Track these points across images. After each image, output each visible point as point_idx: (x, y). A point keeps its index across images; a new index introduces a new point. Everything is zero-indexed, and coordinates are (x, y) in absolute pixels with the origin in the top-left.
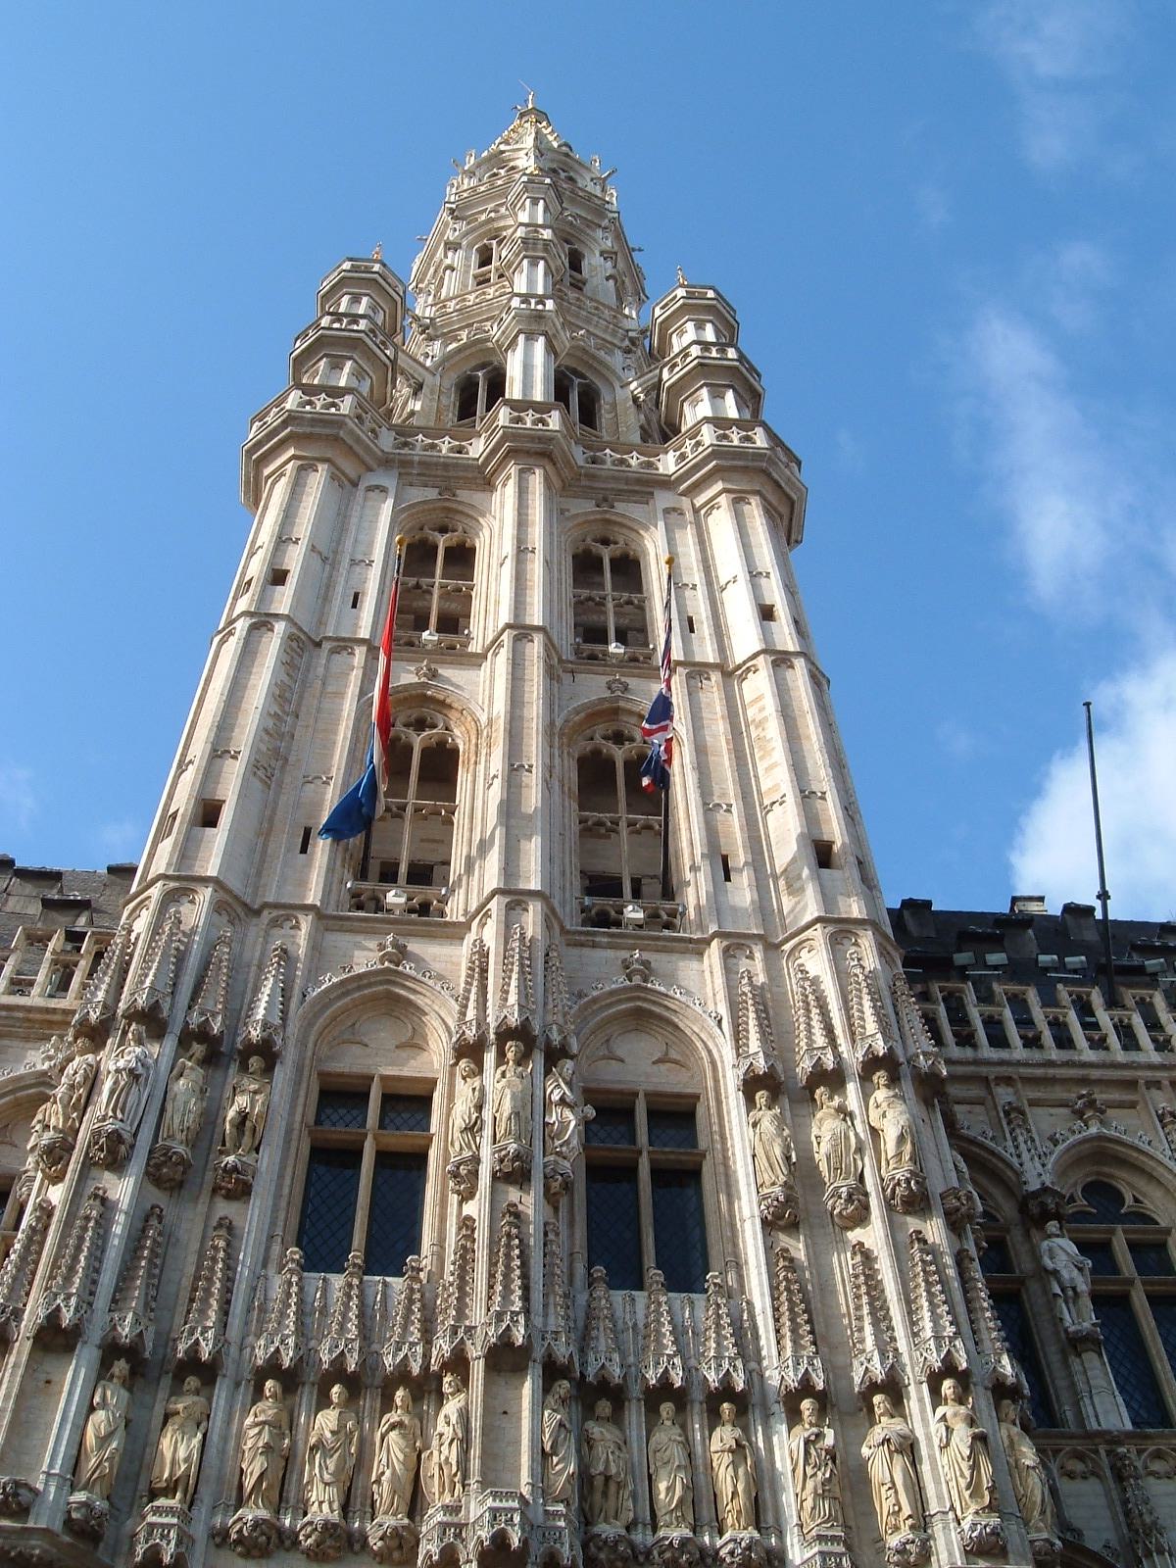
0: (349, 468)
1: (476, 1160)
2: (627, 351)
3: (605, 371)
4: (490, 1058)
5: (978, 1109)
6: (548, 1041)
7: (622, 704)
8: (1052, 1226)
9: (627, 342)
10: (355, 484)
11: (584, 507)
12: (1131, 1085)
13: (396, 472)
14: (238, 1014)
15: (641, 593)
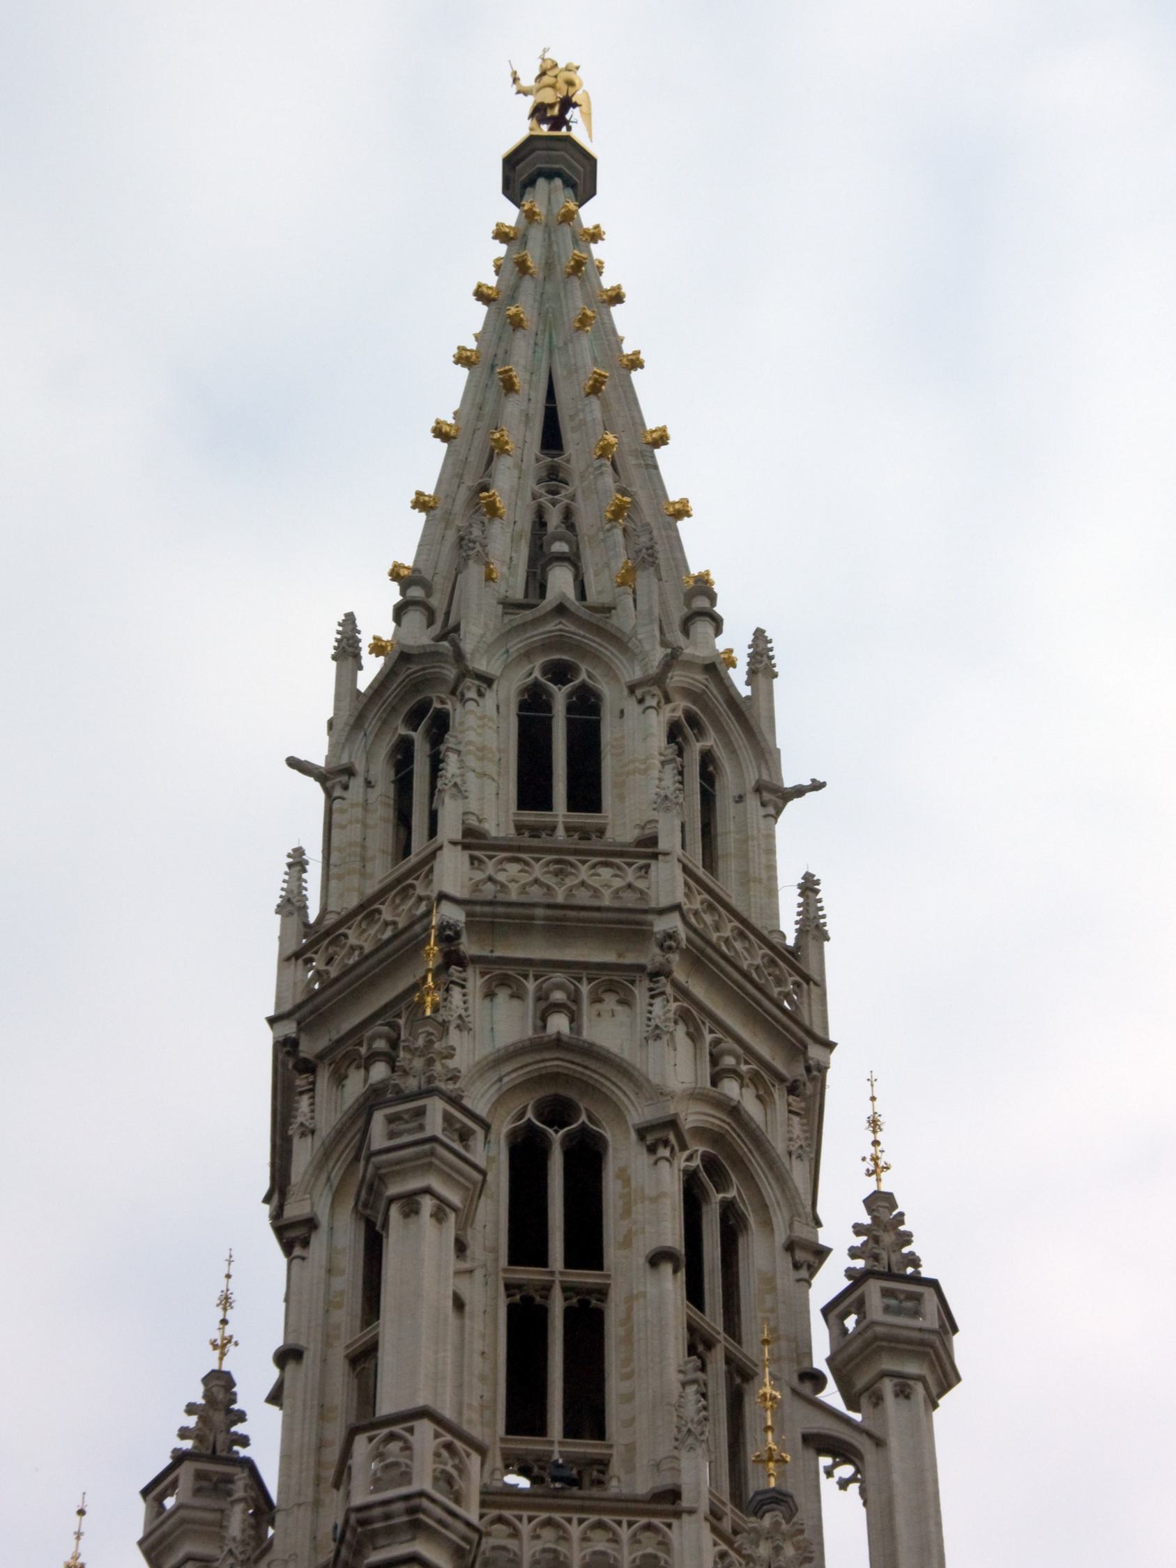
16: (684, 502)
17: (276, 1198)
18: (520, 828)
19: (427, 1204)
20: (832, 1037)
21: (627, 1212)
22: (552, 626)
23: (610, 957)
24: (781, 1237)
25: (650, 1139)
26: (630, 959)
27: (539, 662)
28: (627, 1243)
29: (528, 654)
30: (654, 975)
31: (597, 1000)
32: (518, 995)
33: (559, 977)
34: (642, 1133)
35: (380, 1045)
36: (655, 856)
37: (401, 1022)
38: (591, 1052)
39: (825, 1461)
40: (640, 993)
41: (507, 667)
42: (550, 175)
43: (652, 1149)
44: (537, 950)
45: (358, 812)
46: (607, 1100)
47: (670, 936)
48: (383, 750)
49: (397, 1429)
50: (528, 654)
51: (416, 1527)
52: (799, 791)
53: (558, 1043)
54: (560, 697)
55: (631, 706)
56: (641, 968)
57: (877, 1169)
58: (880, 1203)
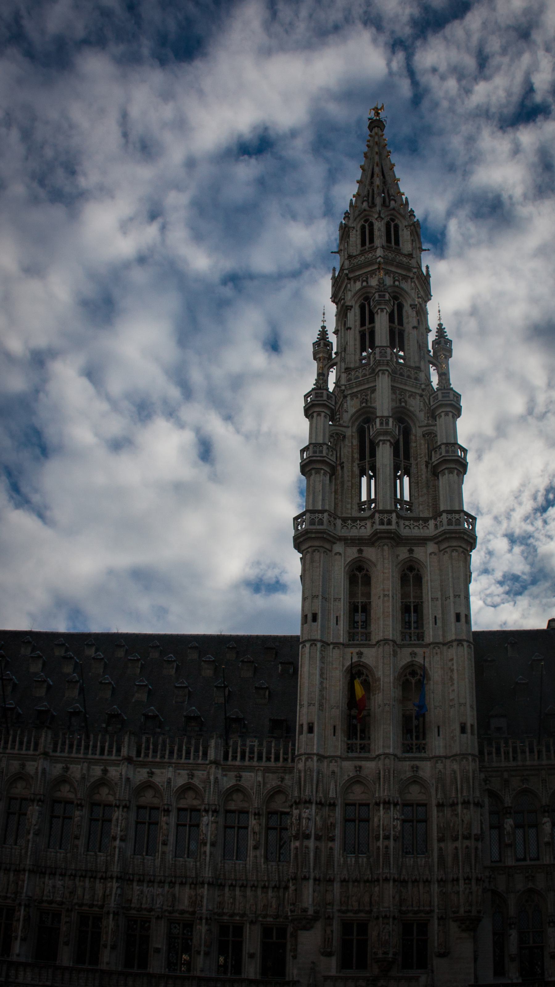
0: (327, 546)
1: (379, 834)
2: (421, 396)
4: (382, 806)
6: (394, 802)
7: (414, 663)
10: (331, 551)
11: (403, 553)
13: (343, 543)
15: (422, 600)
16: (404, 193)
17: (333, 298)
18: (387, 246)
19: (385, 311)
20: (432, 294)
21: (408, 318)
22: (392, 212)
24: (424, 327)
25: (412, 307)
26: (408, 275)
27: (389, 217)
28: (408, 323)
29: (388, 216)
30: (412, 278)
31: (402, 280)
32: (389, 276)
33: (397, 275)
34: (411, 305)
35: (364, 279)
36: (413, 258)
38: (402, 289)
39: (431, 366)
40: (409, 280)
41: (385, 217)
43: (412, 309)
44: (393, 269)
45: (355, 236)
46: (404, 298)
47: (416, 272)
48: (359, 226)
49: (384, 348)
50: (388, 216)
51: (388, 365)
52: (425, 250)
53: (397, 286)
54: (392, 224)
55: (405, 230)
56: (409, 277)
58: (440, 325)
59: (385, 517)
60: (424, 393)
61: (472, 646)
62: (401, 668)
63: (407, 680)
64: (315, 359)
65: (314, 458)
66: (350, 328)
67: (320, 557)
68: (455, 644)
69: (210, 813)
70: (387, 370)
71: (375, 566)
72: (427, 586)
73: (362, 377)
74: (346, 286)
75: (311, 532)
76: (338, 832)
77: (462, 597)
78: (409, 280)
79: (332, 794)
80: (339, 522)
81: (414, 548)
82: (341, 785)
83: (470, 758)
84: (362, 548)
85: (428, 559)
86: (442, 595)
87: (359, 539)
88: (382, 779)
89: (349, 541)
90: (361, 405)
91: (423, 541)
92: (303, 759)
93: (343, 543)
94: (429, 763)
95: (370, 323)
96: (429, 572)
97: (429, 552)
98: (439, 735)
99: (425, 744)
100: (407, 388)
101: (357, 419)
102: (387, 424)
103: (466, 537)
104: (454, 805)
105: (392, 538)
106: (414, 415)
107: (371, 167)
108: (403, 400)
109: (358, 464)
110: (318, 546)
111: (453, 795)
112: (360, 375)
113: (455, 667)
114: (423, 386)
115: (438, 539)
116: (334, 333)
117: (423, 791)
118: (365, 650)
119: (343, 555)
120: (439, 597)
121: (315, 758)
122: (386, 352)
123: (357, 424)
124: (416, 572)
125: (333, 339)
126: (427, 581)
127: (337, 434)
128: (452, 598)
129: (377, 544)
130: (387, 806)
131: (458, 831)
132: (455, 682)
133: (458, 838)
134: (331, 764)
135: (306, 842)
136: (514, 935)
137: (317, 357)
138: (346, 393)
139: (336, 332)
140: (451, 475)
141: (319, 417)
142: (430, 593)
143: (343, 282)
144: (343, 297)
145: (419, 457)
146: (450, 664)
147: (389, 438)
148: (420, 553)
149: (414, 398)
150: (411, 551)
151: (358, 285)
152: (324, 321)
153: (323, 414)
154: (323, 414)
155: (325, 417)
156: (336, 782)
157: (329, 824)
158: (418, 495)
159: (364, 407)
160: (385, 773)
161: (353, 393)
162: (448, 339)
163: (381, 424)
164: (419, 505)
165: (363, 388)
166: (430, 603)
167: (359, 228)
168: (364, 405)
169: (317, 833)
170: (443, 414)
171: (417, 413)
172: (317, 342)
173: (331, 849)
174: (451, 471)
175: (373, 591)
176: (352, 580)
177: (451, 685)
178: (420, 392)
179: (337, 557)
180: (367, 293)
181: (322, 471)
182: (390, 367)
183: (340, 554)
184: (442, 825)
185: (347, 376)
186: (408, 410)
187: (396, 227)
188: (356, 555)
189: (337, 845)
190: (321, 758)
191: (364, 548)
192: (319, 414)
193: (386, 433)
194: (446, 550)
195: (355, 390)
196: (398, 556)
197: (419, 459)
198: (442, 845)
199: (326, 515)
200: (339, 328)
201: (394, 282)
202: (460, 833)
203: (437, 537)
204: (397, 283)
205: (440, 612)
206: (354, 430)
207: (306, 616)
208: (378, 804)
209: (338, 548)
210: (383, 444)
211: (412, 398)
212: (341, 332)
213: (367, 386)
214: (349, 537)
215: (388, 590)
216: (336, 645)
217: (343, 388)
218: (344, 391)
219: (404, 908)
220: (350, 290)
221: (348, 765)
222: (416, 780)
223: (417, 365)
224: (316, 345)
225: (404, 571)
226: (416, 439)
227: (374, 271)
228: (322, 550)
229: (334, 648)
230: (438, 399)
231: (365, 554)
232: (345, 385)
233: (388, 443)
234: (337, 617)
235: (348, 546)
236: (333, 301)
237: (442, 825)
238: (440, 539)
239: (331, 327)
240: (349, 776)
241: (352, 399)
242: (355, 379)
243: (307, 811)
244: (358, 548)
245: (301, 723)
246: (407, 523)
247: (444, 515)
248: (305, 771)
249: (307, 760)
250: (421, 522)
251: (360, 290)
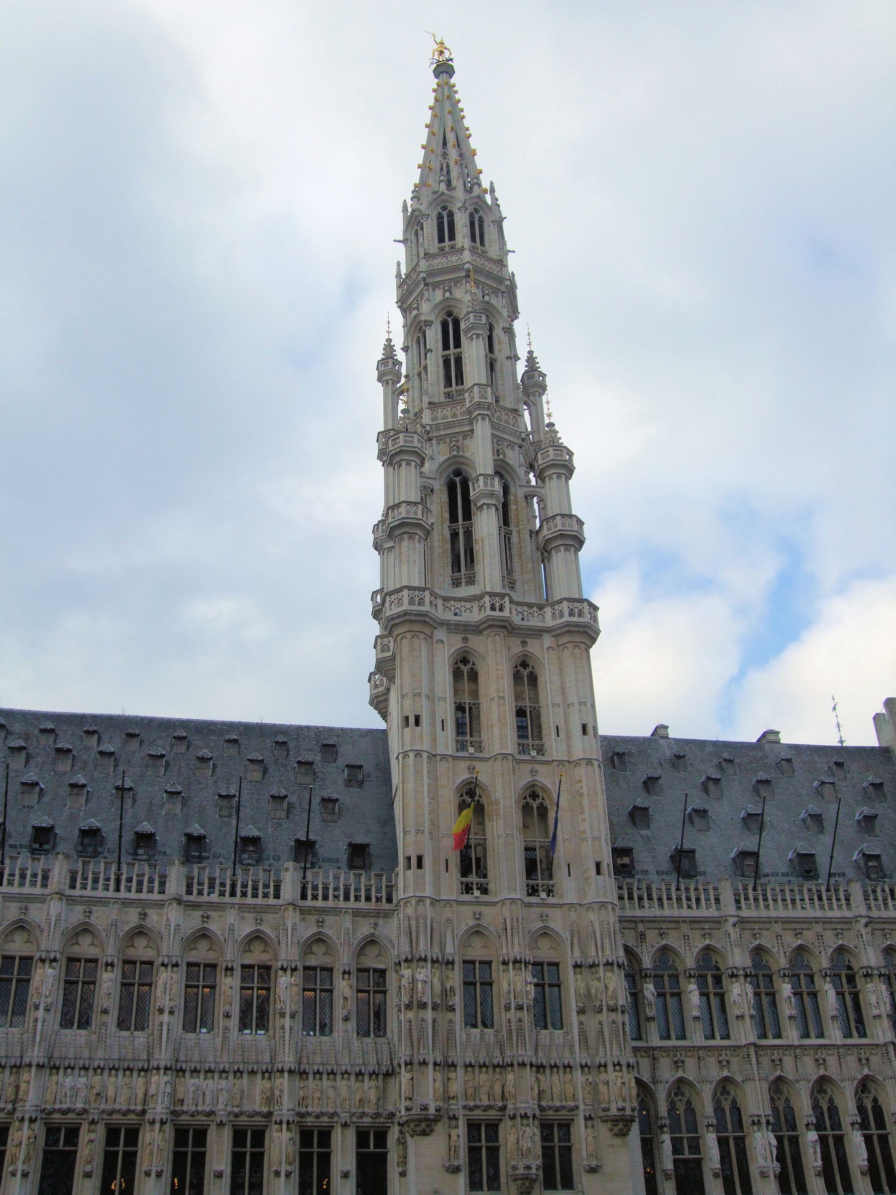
0: (428, 631)
2: (521, 447)
3: (508, 469)
5: (633, 931)
7: (536, 783)
8: (648, 980)
9: (520, 441)
10: (431, 637)
12: (678, 922)
13: (445, 628)
14: (442, 948)
17: (400, 304)
23: (495, 285)
26: (498, 287)
30: (502, 292)
33: (486, 287)
34: (503, 329)
37: (452, 284)
38: (493, 306)
42: (447, 73)
48: (435, 213)
54: (477, 216)
55: (492, 225)
57: (530, 344)
58: (531, 353)
59: (497, 602)
60: (523, 444)
61: (602, 765)
62: (522, 789)
63: (527, 803)
64: (380, 380)
65: (408, 520)
66: (431, 351)
67: (420, 645)
68: (583, 763)
69: (289, 972)
70: (488, 415)
71: (484, 658)
72: (546, 688)
73: (452, 418)
74: (421, 294)
75: (410, 614)
76: (457, 1000)
77: (589, 705)
78: (500, 295)
79: (449, 949)
80: (440, 602)
81: (527, 640)
82: (459, 936)
83: (610, 907)
84: (467, 636)
85: (546, 654)
86: (564, 701)
87: (465, 626)
88: (509, 931)
89: (453, 628)
90: (450, 453)
91: (539, 632)
92: (413, 902)
93: (445, 628)
94: (559, 910)
95: (455, 347)
96: (547, 672)
97: (546, 647)
98: (569, 875)
99: (553, 886)
100: (504, 436)
101: (446, 469)
102: (492, 485)
103: (590, 632)
104: (593, 966)
105: (505, 627)
106: (514, 470)
107: (442, 130)
108: (501, 451)
109: (449, 527)
110: (417, 632)
111: (594, 953)
112: (449, 414)
113: (585, 790)
114: (523, 436)
115: (556, 632)
116: (402, 349)
117: (554, 946)
118: (479, 765)
119: (446, 643)
120: (561, 702)
121: (428, 902)
122: (486, 392)
123: (445, 475)
124: (530, 669)
125: (401, 356)
126: (546, 681)
127: (424, 487)
128: (576, 705)
129: (485, 633)
130: (517, 965)
131: (602, 1001)
132: (586, 808)
133: (602, 1009)
134: (445, 909)
135: (422, 1013)
136: (666, 1139)
137: (384, 379)
138: (430, 435)
139: (405, 349)
140: (567, 553)
141: (408, 467)
142: (549, 698)
143: (417, 285)
144: (416, 305)
145: (521, 523)
146: (578, 786)
147: (494, 502)
148: (534, 647)
149: (513, 449)
150: (524, 643)
151: (438, 296)
152: (389, 332)
153: (413, 464)
154: (413, 464)
155: (416, 467)
156: (453, 933)
157: (449, 988)
158: (522, 571)
159: (455, 456)
160: (512, 923)
161: (441, 435)
162: (540, 372)
163: (485, 484)
164: (523, 584)
165: (453, 431)
166: (551, 710)
167: (435, 218)
168: (455, 453)
169: (434, 1001)
170: (554, 476)
171: (516, 467)
172: (383, 359)
173: (451, 1021)
174: (567, 547)
175: (482, 690)
176: (457, 675)
177: (581, 813)
178: (520, 441)
179: (439, 645)
180: (450, 306)
181: (417, 537)
182: (490, 411)
183: (442, 642)
184: (582, 992)
185: (432, 413)
186: (507, 464)
187: (481, 220)
188: (460, 645)
189: (458, 1017)
190: (434, 902)
191: (470, 637)
192: (408, 463)
193: (492, 495)
194: (567, 645)
195: (442, 433)
196: (509, 648)
197: (521, 527)
198: (583, 1018)
199: (427, 593)
200: (410, 345)
201: (483, 297)
202: (604, 1003)
203: (556, 629)
204: (487, 298)
205: (563, 721)
206: (442, 483)
207: (407, 718)
208: (505, 963)
209: (440, 634)
210: (487, 508)
211: (509, 448)
212: (412, 350)
213: (457, 430)
214: (453, 622)
215: (504, 692)
216: (444, 757)
217: (428, 428)
218: (429, 433)
219: (544, 1103)
220: (428, 300)
221: (467, 911)
222: (545, 933)
223: (514, 407)
224: (382, 364)
225: (516, 667)
226: (516, 501)
227: (459, 279)
228: (422, 636)
229: (441, 760)
230: (548, 456)
231: (470, 644)
232: (430, 425)
233: (494, 508)
234: (443, 720)
235: (451, 633)
236: (400, 307)
237: (582, 992)
238: (559, 632)
239: (398, 341)
240: (467, 924)
241: (438, 443)
242: (442, 419)
243: (422, 971)
244: (463, 635)
245: (407, 855)
246: (519, 609)
247: (565, 604)
248: (417, 919)
249: (417, 903)
250: (535, 609)
251: (441, 302)
